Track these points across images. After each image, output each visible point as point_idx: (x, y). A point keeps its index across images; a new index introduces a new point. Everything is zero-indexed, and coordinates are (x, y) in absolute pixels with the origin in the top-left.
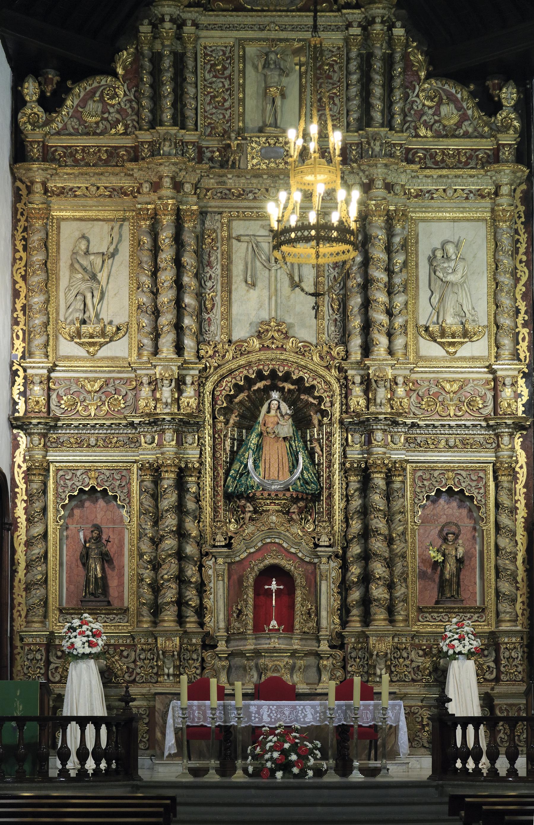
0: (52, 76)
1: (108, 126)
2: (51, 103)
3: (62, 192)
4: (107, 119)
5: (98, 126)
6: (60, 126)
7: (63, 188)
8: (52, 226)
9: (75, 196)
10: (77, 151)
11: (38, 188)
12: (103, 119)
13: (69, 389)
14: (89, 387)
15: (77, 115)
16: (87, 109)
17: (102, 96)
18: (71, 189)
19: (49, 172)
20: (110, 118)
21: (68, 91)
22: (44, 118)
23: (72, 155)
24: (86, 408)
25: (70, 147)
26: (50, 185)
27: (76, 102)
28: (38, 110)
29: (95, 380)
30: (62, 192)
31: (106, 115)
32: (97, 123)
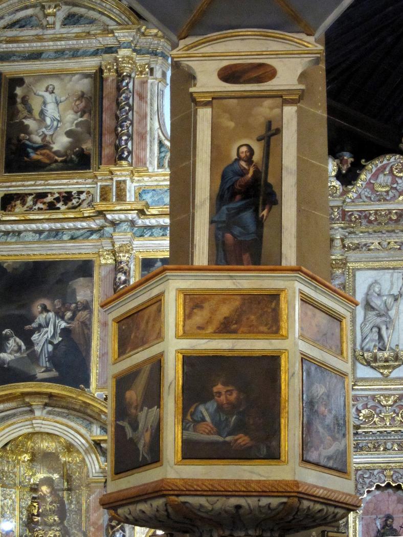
0: (348, 157)
1: (397, 194)
2: (347, 178)
3: (357, 247)
4: (395, 188)
5: (388, 194)
6: (355, 195)
7: (359, 244)
8: (349, 275)
9: (369, 250)
10: (370, 214)
11: (338, 243)
12: (392, 188)
13: (367, 404)
14: (384, 403)
15: (370, 185)
16: (379, 181)
17: (391, 171)
18: (365, 245)
19: (348, 230)
20: (398, 188)
21: (363, 167)
22: (341, 190)
23: (366, 217)
24: (382, 420)
25: (365, 211)
26: (347, 242)
27: (369, 176)
28: (336, 183)
29: (387, 397)
30: (357, 247)
31: (395, 186)
32: (387, 192)
